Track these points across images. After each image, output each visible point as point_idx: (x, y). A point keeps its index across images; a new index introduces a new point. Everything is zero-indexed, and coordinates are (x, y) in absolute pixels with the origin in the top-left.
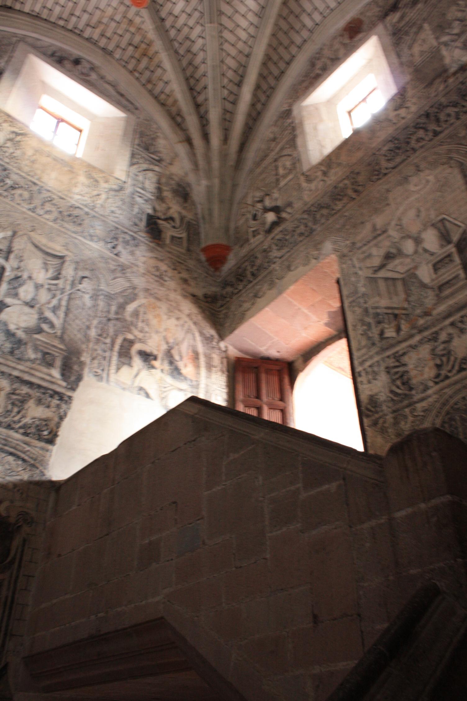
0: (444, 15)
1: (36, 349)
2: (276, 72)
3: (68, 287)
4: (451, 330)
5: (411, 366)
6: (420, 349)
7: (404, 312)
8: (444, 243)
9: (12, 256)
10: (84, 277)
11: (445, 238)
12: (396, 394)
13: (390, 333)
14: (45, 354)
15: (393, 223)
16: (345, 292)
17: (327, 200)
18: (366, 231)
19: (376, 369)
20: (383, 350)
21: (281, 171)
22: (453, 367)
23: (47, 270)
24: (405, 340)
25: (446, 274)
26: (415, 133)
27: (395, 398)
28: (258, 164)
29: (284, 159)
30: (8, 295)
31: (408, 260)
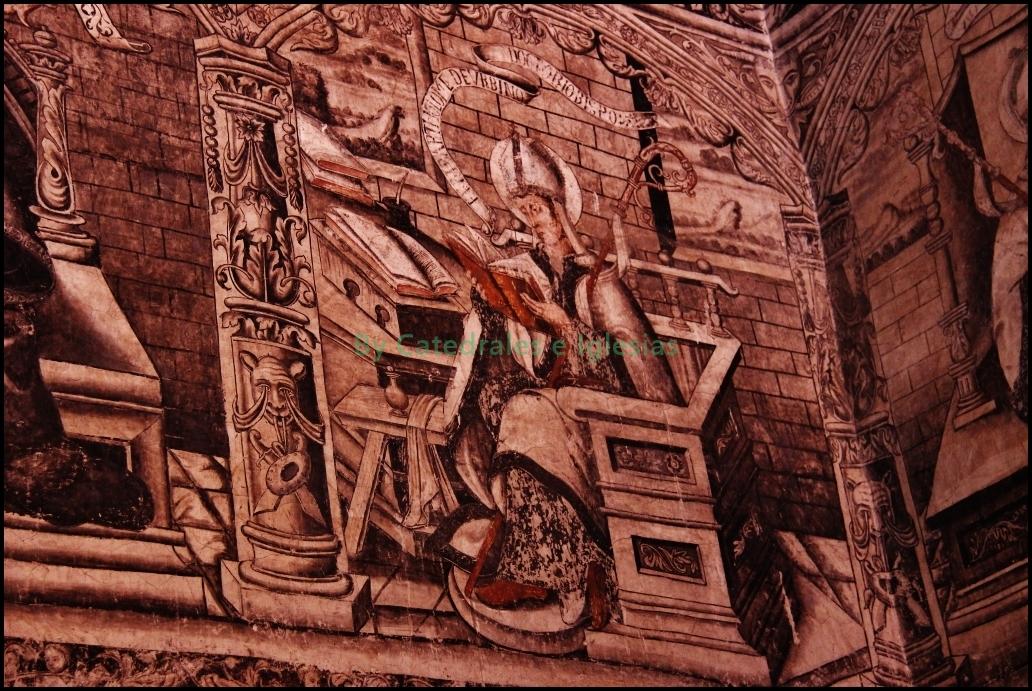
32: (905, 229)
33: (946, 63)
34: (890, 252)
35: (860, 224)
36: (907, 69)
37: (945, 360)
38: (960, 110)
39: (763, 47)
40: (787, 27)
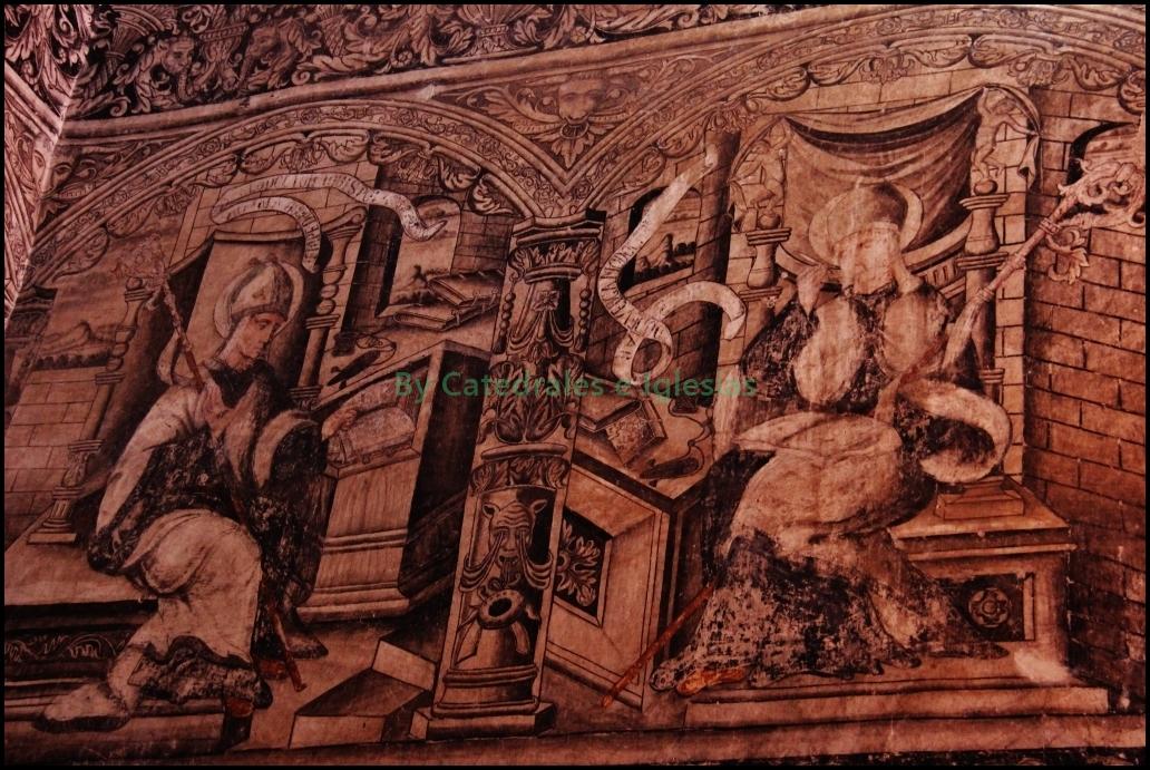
1: (915, 589)
3: (1015, 230)
9: (737, 245)
10: (1079, 146)
14: (959, 595)
23: (899, 217)
30: (751, 412)
32: (87, 352)
33: (198, 237)
34: (64, 363)
35: (52, 327)
36: (164, 222)
37: (55, 479)
38: (188, 281)
39: (52, 128)
40: (83, 126)
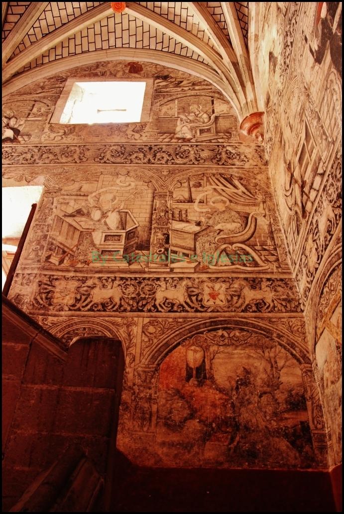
0: (189, 106)
2: (72, 50)
4: (96, 281)
5: (57, 290)
6: (70, 282)
7: (71, 252)
8: (120, 227)
11: (123, 224)
12: (38, 302)
13: (55, 260)
15: (94, 194)
16: (36, 216)
17: (57, 150)
18: (73, 187)
19: (32, 278)
20: (44, 269)
21: (35, 110)
22: (87, 305)
24: (62, 271)
25: (111, 245)
26: (137, 152)
27: (35, 305)
28: (20, 93)
29: (43, 104)
31: (92, 223)
